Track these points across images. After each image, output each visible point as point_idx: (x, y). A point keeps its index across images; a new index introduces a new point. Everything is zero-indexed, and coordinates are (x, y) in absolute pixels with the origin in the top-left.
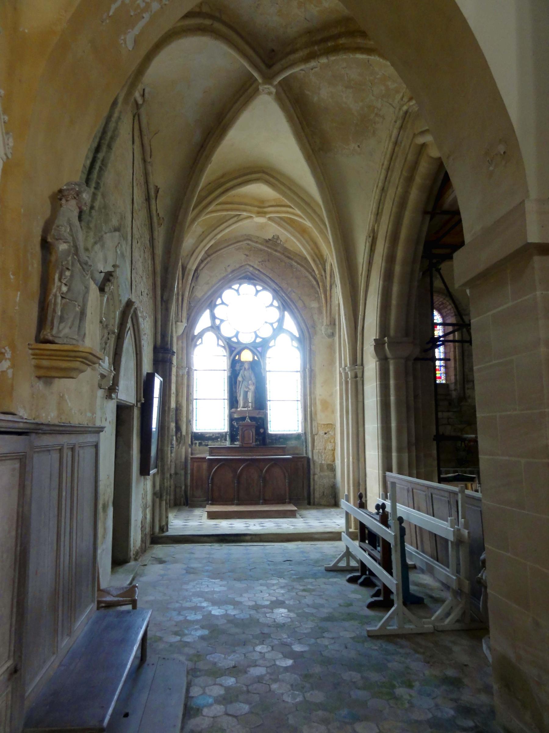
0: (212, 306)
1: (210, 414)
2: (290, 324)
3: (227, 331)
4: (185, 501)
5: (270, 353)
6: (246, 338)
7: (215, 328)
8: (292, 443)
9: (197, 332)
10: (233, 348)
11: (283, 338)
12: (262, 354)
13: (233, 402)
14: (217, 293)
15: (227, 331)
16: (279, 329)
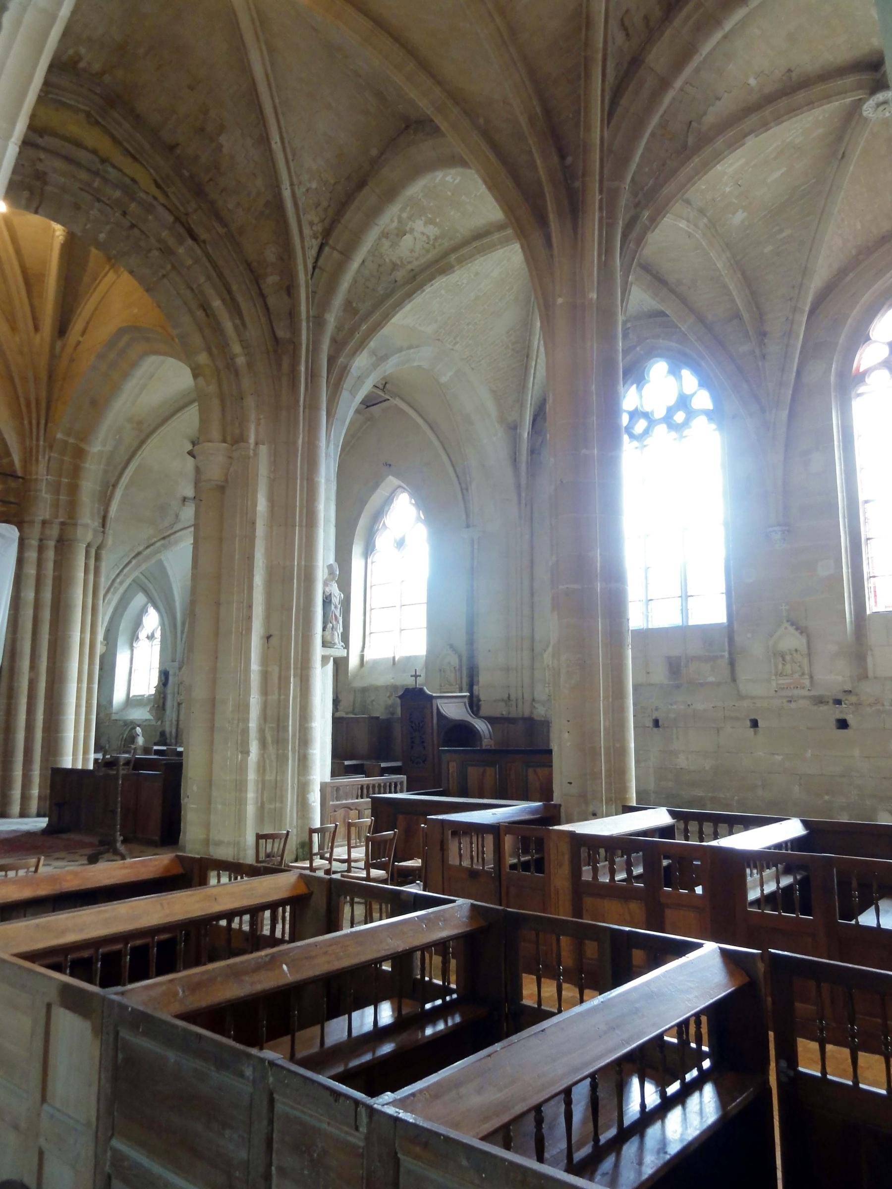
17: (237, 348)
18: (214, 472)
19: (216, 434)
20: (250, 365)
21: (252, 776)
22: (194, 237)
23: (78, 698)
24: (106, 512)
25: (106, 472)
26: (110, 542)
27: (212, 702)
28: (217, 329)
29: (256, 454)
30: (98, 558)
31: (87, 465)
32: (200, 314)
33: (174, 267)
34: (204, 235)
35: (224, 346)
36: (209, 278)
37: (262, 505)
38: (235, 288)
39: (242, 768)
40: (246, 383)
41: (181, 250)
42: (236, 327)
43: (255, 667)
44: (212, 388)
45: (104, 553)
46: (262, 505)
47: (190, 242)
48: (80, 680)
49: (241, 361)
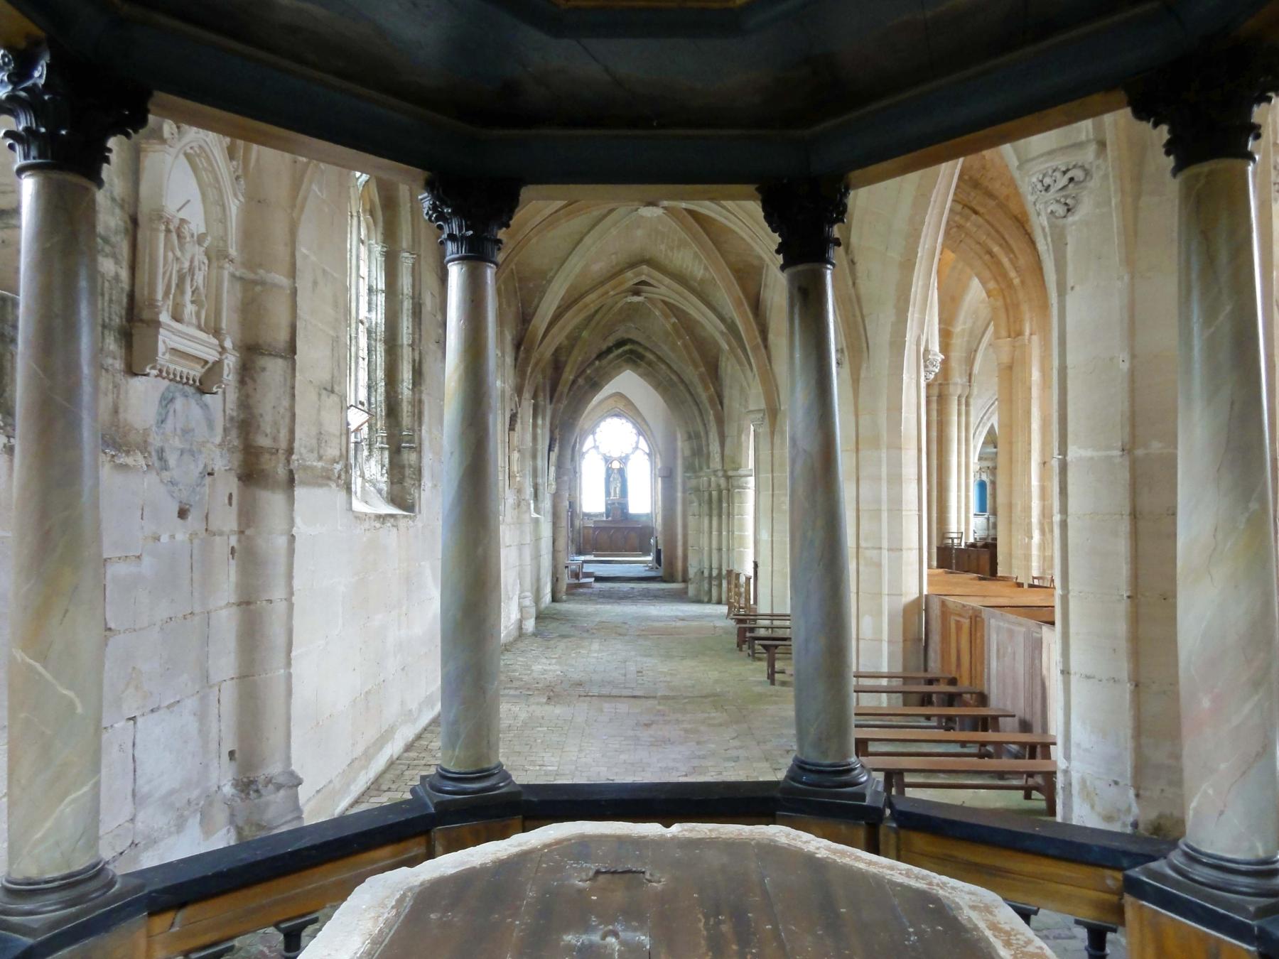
0: (594, 433)
1: (593, 500)
2: (643, 444)
3: (603, 450)
4: (580, 553)
5: (629, 464)
6: (616, 454)
7: (596, 447)
8: (644, 519)
9: (584, 449)
10: (608, 460)
11: (638, 452)
12: (625, 464)
13: (608, 493)
14: (597, 425)
15: (603, 450)
16: (637, 448)
17: (1013, 274)
18: (1005, 359)
19: (1004, 333)
20: (1023, 282)
21: (1035, 552)
22: (976, 212)
23: (959, 502)
24: (971, 369)
25: (969, 342)
26: (975, 391)
27: (1010, 506)
28: (999, 264)
29: (1030, 341)
30: (967, 405)
31: (954, 341)
32: (987, 257)
33: (967, 234)
34: (981, 210)
35: (1004, 275)
36: (989, 235)
37: (1036, 375)
38: (1007, 237)
39: (1028, 547)
40: (1021, 295)
41: (968, 224)
42: (1010, 260)
43: (1035, 482)
44: (1000, 303)
45: (972, 401)
46: (1036, 375)
47: (974, 216)
48: (959, 490)
49: (1017, 281)
